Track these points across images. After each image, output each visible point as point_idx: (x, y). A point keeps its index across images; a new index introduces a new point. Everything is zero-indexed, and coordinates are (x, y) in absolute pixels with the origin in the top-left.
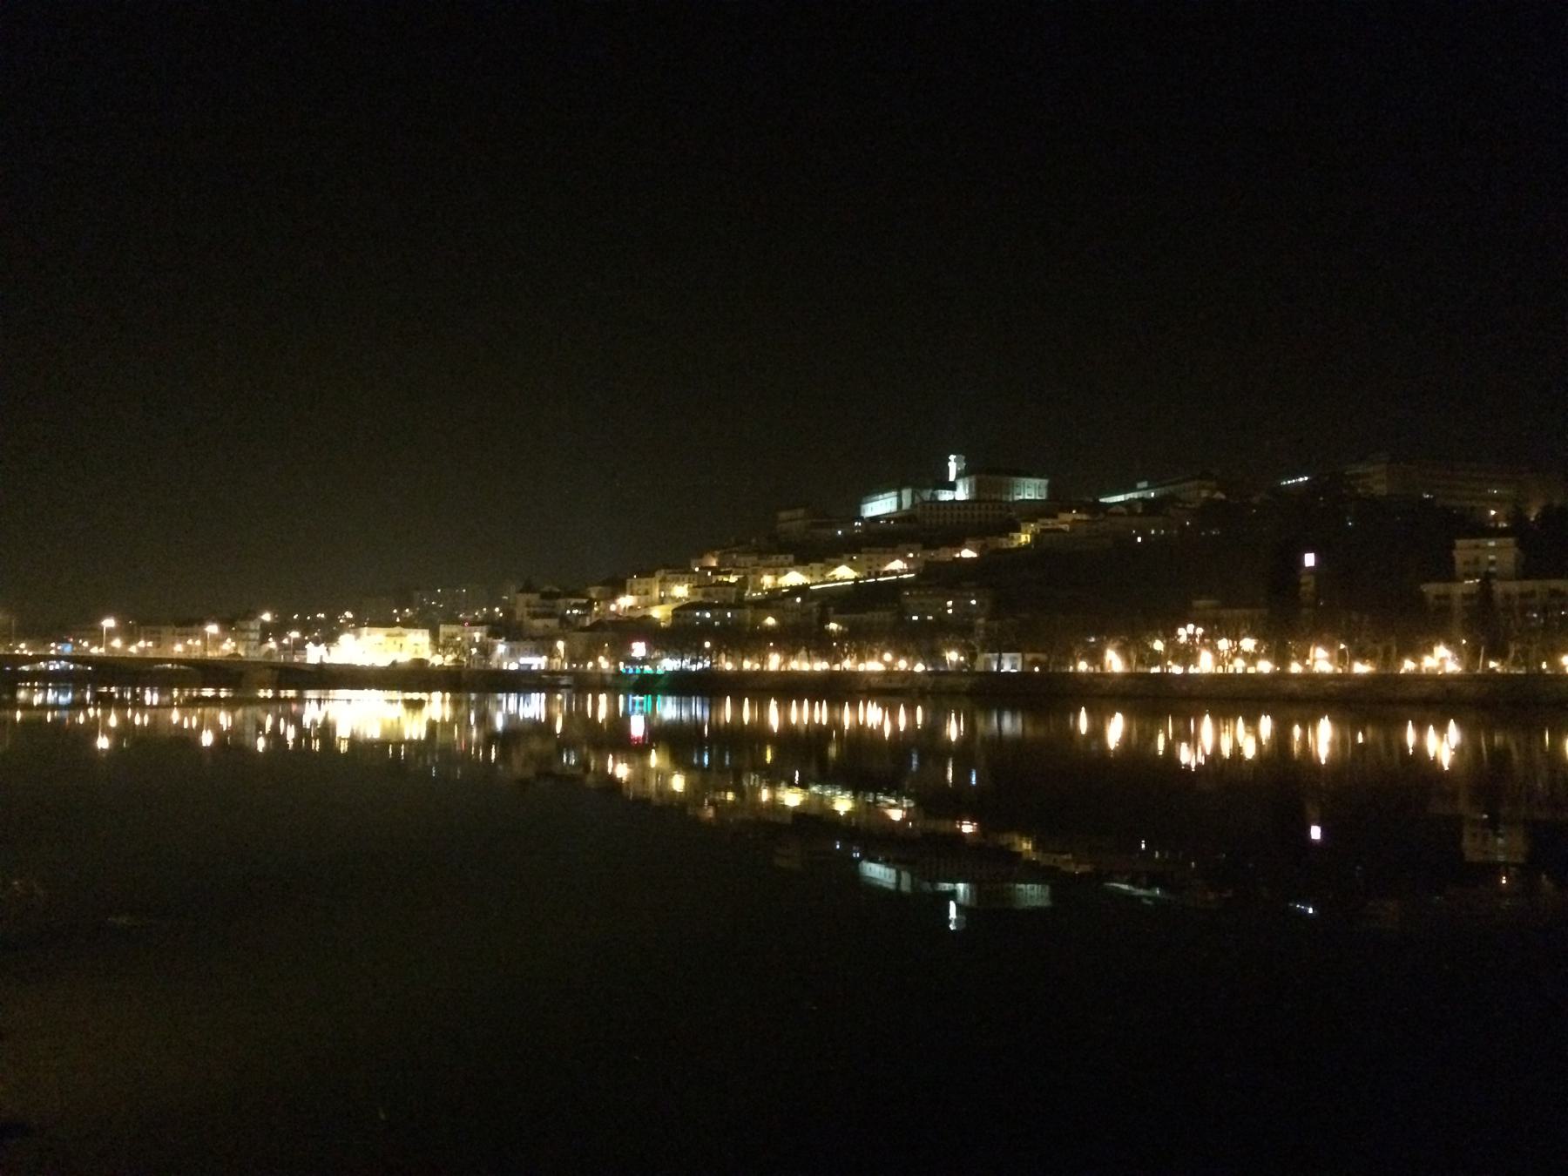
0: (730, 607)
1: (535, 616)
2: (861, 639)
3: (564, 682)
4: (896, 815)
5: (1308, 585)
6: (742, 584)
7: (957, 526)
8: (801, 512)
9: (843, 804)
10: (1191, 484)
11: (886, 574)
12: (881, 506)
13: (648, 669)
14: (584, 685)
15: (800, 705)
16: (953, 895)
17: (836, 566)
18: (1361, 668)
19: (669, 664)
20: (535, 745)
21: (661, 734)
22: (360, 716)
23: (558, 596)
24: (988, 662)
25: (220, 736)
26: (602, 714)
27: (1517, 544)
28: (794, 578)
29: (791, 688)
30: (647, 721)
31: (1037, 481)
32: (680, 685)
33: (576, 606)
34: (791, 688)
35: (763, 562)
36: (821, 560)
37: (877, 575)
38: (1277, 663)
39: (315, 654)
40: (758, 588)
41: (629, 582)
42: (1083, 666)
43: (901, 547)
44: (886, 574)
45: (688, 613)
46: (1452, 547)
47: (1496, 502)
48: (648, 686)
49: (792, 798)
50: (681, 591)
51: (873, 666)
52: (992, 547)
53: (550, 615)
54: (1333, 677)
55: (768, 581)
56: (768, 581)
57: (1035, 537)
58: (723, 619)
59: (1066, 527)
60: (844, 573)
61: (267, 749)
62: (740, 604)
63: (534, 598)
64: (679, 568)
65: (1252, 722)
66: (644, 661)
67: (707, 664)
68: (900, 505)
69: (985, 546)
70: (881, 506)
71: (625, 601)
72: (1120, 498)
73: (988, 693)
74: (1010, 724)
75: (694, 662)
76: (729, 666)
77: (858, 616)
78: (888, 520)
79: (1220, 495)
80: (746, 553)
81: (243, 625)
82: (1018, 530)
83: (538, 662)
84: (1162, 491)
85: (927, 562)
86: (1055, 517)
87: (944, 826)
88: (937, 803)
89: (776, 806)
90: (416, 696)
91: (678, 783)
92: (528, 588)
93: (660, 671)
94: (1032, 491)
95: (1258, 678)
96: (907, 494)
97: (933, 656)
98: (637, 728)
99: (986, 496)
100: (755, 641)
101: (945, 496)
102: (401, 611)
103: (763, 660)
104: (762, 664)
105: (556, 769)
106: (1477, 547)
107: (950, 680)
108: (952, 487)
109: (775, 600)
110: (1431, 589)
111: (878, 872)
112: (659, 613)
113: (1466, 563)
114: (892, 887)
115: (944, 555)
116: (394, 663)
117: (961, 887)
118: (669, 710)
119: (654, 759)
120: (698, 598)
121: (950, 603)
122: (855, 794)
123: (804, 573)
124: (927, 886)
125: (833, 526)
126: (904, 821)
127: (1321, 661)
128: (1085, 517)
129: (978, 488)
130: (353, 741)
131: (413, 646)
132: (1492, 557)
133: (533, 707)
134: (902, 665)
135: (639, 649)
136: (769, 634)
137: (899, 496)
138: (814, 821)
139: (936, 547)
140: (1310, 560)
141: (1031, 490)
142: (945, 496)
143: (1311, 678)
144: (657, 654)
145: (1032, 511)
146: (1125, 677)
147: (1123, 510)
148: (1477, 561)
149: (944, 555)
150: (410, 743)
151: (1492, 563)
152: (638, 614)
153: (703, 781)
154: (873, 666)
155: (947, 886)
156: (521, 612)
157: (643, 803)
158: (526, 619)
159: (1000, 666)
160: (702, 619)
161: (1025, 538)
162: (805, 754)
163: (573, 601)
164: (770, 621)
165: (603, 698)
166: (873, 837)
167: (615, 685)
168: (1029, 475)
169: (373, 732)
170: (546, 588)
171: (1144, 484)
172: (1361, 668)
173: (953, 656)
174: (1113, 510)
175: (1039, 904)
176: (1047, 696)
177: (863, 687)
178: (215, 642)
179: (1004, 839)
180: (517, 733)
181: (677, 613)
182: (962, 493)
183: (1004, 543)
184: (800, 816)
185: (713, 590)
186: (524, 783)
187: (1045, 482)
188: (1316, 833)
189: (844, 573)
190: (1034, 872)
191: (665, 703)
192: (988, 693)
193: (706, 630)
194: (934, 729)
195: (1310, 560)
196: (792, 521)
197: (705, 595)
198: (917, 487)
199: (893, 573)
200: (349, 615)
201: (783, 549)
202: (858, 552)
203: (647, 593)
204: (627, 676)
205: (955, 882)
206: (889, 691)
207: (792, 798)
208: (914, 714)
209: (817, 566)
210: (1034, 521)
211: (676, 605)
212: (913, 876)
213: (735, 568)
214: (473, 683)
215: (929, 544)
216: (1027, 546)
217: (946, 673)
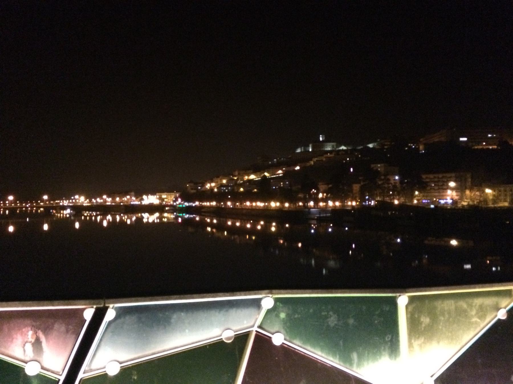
1: (192, 189)
13: (181, 206)
19: (187, 204)
25: (109, 222)
28: (252, 177)
31: (333, 144)
32: (188, 210)
37: (275, 175)
50: (224, 181)
53: (195, 189)
55: (246, 178)
56: (246, 178)
59: (324, 159)
61: (80, 227)
63: (192, 184)
64: (225, 176)
71: (213, 184)
93: (184, 206)
94: (331, 146)
96: (303, 148)
115: (291, 169)
118: (187, 216)
147: (344, 153)
149: (291, 169)
160: (223, 190)
164: (242, 189)
183: (308, 164)
199: (279, 174)
209: (259, 173)
210: (316, 157)
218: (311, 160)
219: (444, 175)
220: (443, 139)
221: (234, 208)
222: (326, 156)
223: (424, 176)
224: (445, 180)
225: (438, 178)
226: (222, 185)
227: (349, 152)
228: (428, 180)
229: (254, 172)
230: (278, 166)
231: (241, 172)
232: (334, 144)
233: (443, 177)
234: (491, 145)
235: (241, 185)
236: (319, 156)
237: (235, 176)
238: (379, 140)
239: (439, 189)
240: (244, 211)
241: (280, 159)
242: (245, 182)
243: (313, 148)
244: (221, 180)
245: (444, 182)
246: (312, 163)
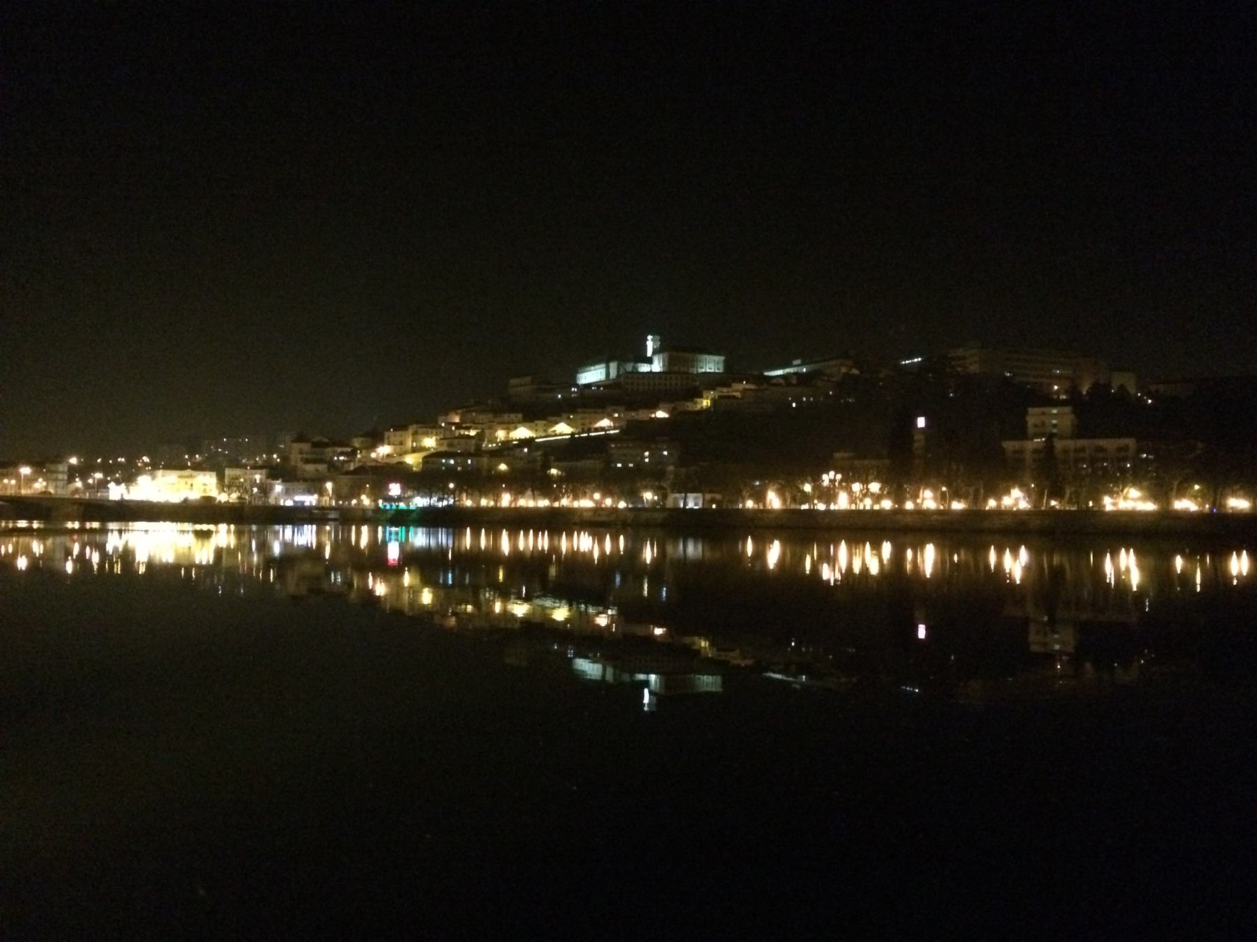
0: (470, 455)
1: (307, 461)
2: (576, 482)
3: (332, 516)
4: (602, 621)
5: (919, 442)
6: (480, 437)
7: (653, 391)
8: (528, 379)
9: (561, 613)
10: (834, 362)
11: (597, 430)
12: (593, 375)
13: (402, 505)
14: (348, 518)
15: (526, 535)
16: (646, 683)
18: (958, 506)
19: (420, 502)
20: (307, 567)
21: (412, 558)
22: (156, 544)
23: (327, 445)
24: (676, 500)
26: (364, 542)
27: (1074, 412)
28: (522, 433)
29: (519, 521)
30: (401, 546)
31: (717, 358)
32: (429, 519)
33: (342, 454)
34: (519, 521)
35: (498, 420)
36: (544, 418)
37: (589, 431)
38: (895, 502)
39: (116, 492)
40: (493, 440)
41: (387, 434)
42: (750, 504)
43: (609, 409)
44: (597, 430)
45: (435, 460)
46: (1026, 413)
47: (1058, 379)
48: (402, 519)
50: (430, 442)
51: (585, 503)
52: (680, 409)
53: (320, 461)
54: (938, 512)
55: (501, 434)
56: (501, 434)
57: (714, 401)
58: (465, 465)
59: (738, 394)
60: (563, 429)
62: (478, 453)
63: (306, 447)
64: (428, 423)
65: (877, 547)
66: (399, 499)
67: (451, 501)
68: (608, 374)
69: (674, 409)
70: (593, 375)
71: (384, 450)
72: (780, 372)
73: (676, 525)
74: (693, 550)
75: (440, 499)
76: (468, 503)
77: (574, 464)
78: (599, 387)
79: (855, 371)
80: (483, 412)
81: (53, 467)
82: (701, 397)
83: (310, 500)
84: (813, 367)
86: (729, 386)
87: (639, 630)
88: (634, 611)
89: (506, 615)
90: (205, 527)
92: (300, 439)
93: (412, 507)
94: (712, 365)
95: (880, 513)
96: (613, 366)
97: (633, 495)
98: (393, 553)
99: (676, 368)
100: (491, 483)
101: (644, 368)
102: (192, 455)
103: (497, 498)
104: (496, 502)
105: (325, 586)
106: (1044, 414)
107: (644, 516)
108: (650, 361)
109: (506, 450)
110: (1010, 445)
111: (589, 668)
112: (412, 460)
113: (1036, 426)
114: (599, 678)
115: (642, 415)
116: (186, 500)
117: (653, 677)
118: (419, 538)
119: (407, 579)
120: (444, 449)
121: (647, 454)
122: (570, 605)
123: (530, 428)
124: (626, 677)
125: (552, 390)
126: (608, 626)
127: (928, 500)
128: (752, 387)
129: (670, 363)
130: (150, 565)
131: (202, 485)
132: (1054, 422)
133: (306, 536)
134: (608, 502)
135: (395, 489)
136: (502, 477)
138: (538, 628)
139: (636, 409)
140: (921, 422)
142: (644, 368)
143: (920, 513)
144: (409, 493)
145: (712, 381)
146: (784, 511)
147: (782, 381)
148: (1043, 424)
149: (642, 415)
150: (200, 567)
151: (1055, 426)
152: (394, 461)
153: (446, 595)
154: (585, 503)
155: (642, 677)
156: (295, 458)
157: (397, 613)
158: (300, 464)
159: (685, 504)
160: (447, 465)
161: (706, 403)
162: (531, 574)
163: (339, 450)
165: (365, 529)
166: (582, 638)
167: (374, 518)
169: (168, 557)
170: (317, 439)
171: (798, 362)
172: (958, 506)
173: (648, 496)
174: (774, 381)
175: (714, 689)
176: (721, 527)
177: (576, 519)
178: (28, 481)
179: (687, 640)
180: (292, 558)
181: (426, 460)
182: (657, 366)
183: (690, 406)
184: (526, 622)
185: (456, 441)
186: (295, 599)
187: (722, 358)
188: (922, 632)
189: (563, 429)
190: (711, 666)
191: (416, 533)
192: (676, 525)
193: (451, 474)
194: (634, 553)
195: (921, 422)
196: (520, 386)
197: (450, 445)
198: (622, 360)
199: (602, 429)
200: (146, 459)
201: (513, 409)
202: (572, 413)
203: (401, 443)
204: (385, 511)
205: (648, 673)
206: (597, 524)
207: (520, 610)
209: (541, 423)
210: (713, 389)
211: (424, 454)
212: (615, 667)
213: (474, 424)
214: (253, 517)
215: (631, 406)
216: (708, 409)
217: (644, 509)
227: (794, 382)
231: (482, 418)
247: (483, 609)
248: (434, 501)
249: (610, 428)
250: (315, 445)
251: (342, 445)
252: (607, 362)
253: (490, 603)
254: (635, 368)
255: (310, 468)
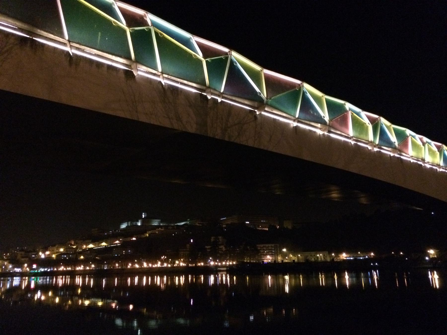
1: (23, 257)
6: (77, 248)
8: (97, 229)
11: (114, 244)
12: (124, 226)
13: (36, 271)
17: (102, 243)
18: (169, 266)
19: (42, 270)
28: (91, 246)
31: (158, 220)
33: (33, 255)
36: (98, 241)
40: (81, 248)
44: (114, 244)
48: (36, 275)
49: (87, 303)
50: (62, 250)
56: (85, 246)
59: (157, 232)
60: (104, 244)
63: (23, 253)
64: (62, 244)
65: (162, 277)
66: (34, 269)
70: (124, 226)
71: (48, 253)
72: (183, 223)
76: (55, 269)
83: (18, 270)
85: (124, 241)
88: (123, 302)
89: (83, 304)
91: (57, 300)
92: (22, 250)
93: (39, 271)
94: (157, 222)
96: (129, 223)
98: (32, 286)
100: (75, 262)
109: (84, 252)
111: (119, 322)
112: (54, 256)
115: (128, 239)
120: (65, 252)
122: (102, 301)
137: (128, 224)
138: (92, 307)
141: (155, 223)
143: (179, 267)
149: (128, 239)
156: (19, 257)
160: (64, 257)
168: (156, 219)
175: (154, 327)
180: (13, 289)
181: (57, 256)
183: (143, 236)
185: (68, 250)
189: (104, 244)
197: (67, 251)
198: (132, 221)
199: (116, 244)
203: (53, 251)
207: (87, 303)
208: (142, 279)
209: (97, 243)
218: (146, 233)
219: (265, 245)
220: (236, 221)
221: (122, 269)
222: (157, 229)
223: (257, 245)
224: (265, 248)
225: (260, 247)
226: (62, 254)
228: (259, 248)
229: (93, 242)
230: (116, 236)
232: (160, 220)
233: (264, 247)
234: (264, 228)
235: (81, 254)
236: (153, 229)
237: (74, 245)
238: (188, 220)
239: (261, 255)
240: (141, 270)
241: (115, 231)
242: (85, 250)
243: (142, 223)
244: (58, 248)
245: (264, 250)
246: (148, 235)
247: (75, 303)
248: (52, 269)
249: (119, 243)
250: (27, 252)
251: (34, 251)
252: (128, 222)
253: (77, 301)
254: (136, 224)
255: (23, 259)
